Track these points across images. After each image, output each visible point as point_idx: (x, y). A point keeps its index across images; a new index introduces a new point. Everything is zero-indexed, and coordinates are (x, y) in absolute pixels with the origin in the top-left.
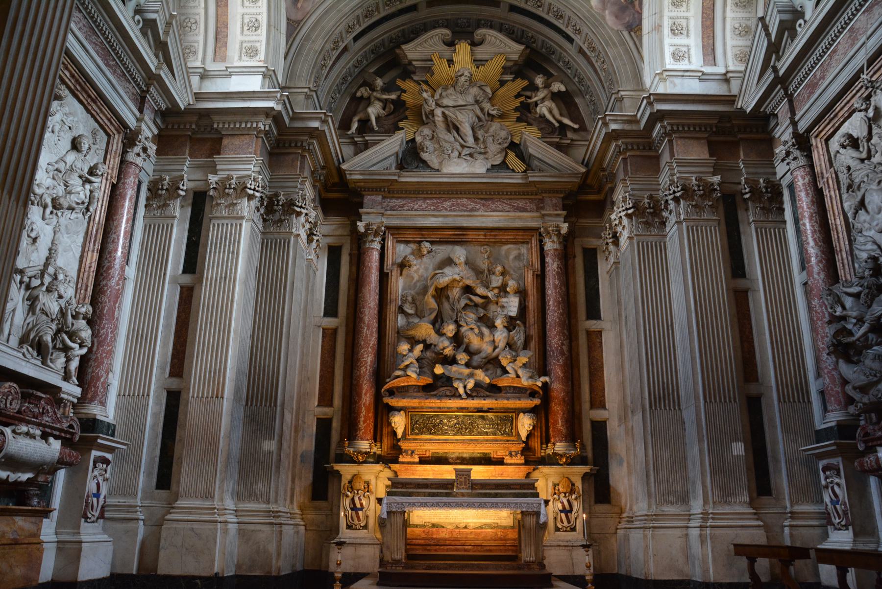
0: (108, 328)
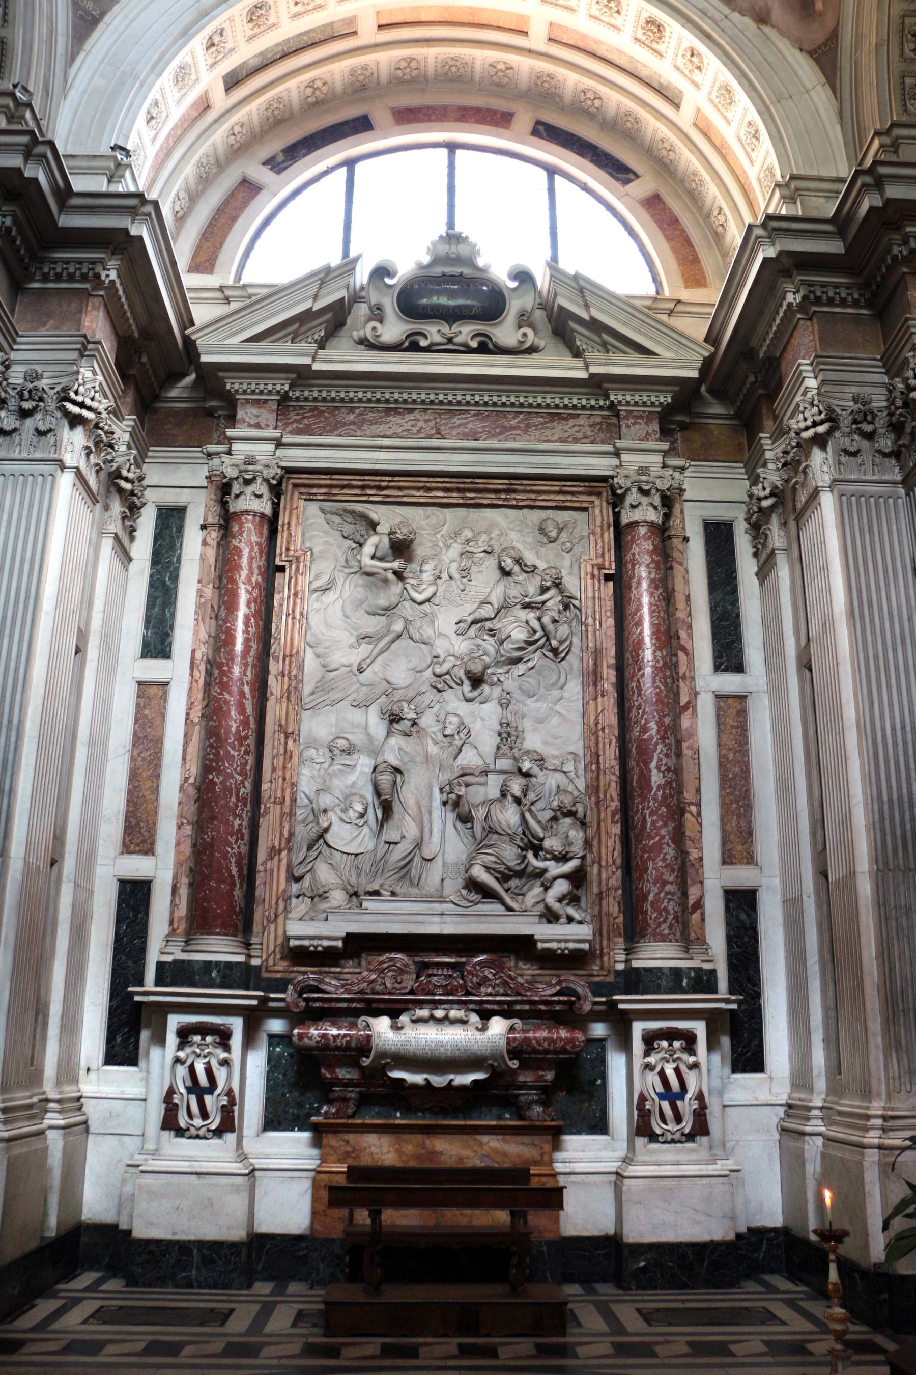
0: (643, 809)
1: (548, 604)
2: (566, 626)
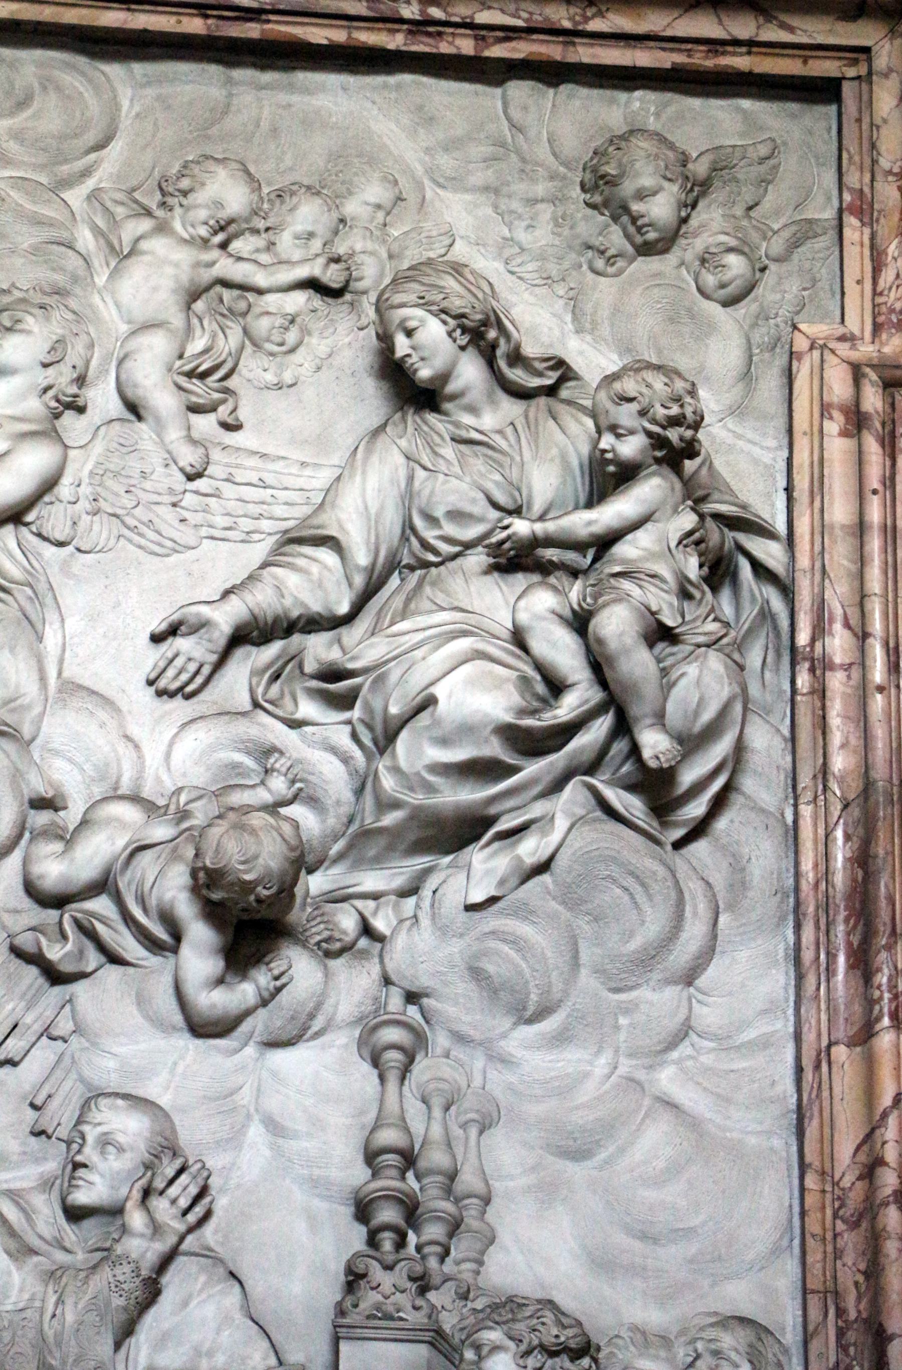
1: (625, 550)
2: (715, 662)
